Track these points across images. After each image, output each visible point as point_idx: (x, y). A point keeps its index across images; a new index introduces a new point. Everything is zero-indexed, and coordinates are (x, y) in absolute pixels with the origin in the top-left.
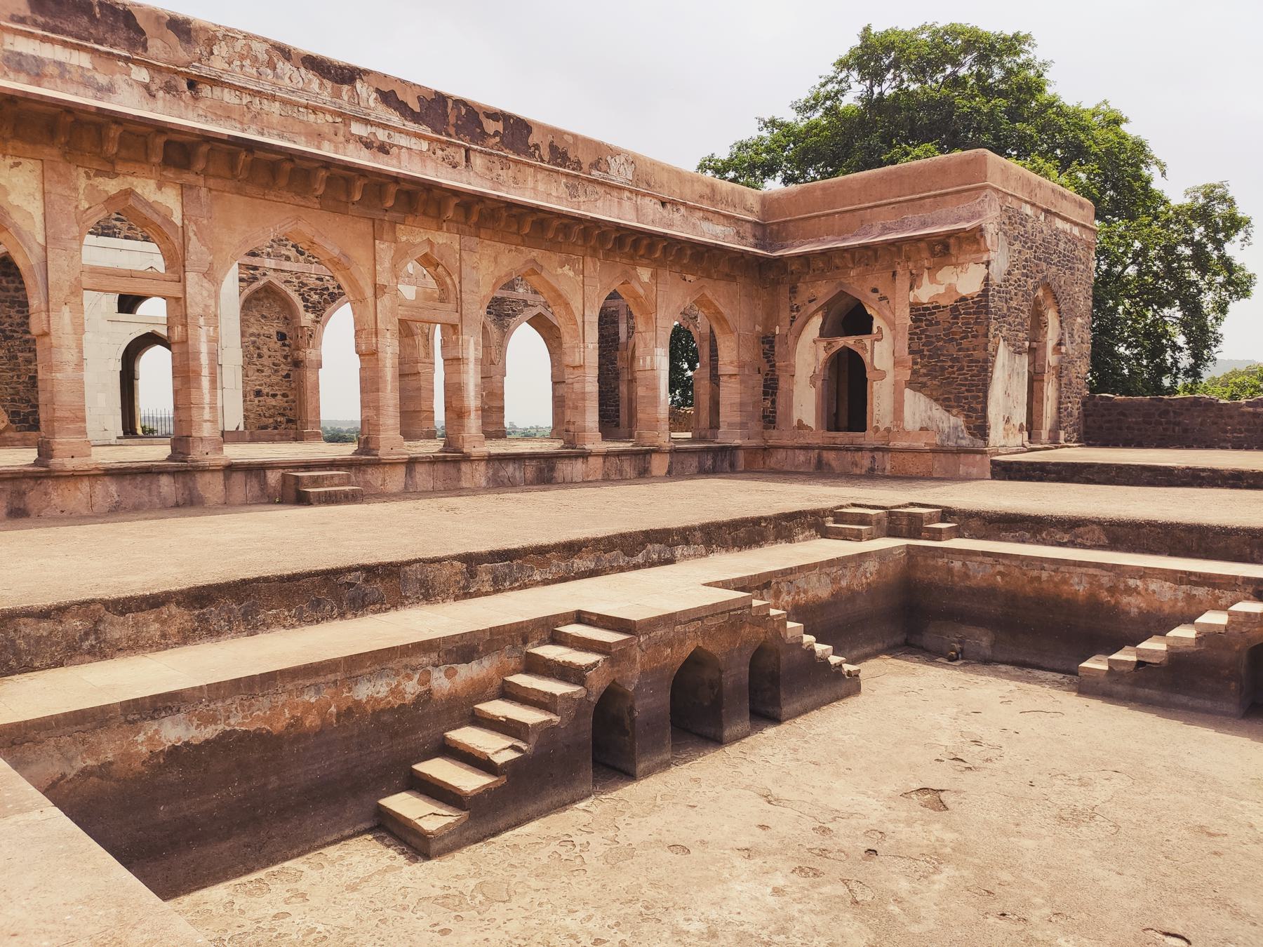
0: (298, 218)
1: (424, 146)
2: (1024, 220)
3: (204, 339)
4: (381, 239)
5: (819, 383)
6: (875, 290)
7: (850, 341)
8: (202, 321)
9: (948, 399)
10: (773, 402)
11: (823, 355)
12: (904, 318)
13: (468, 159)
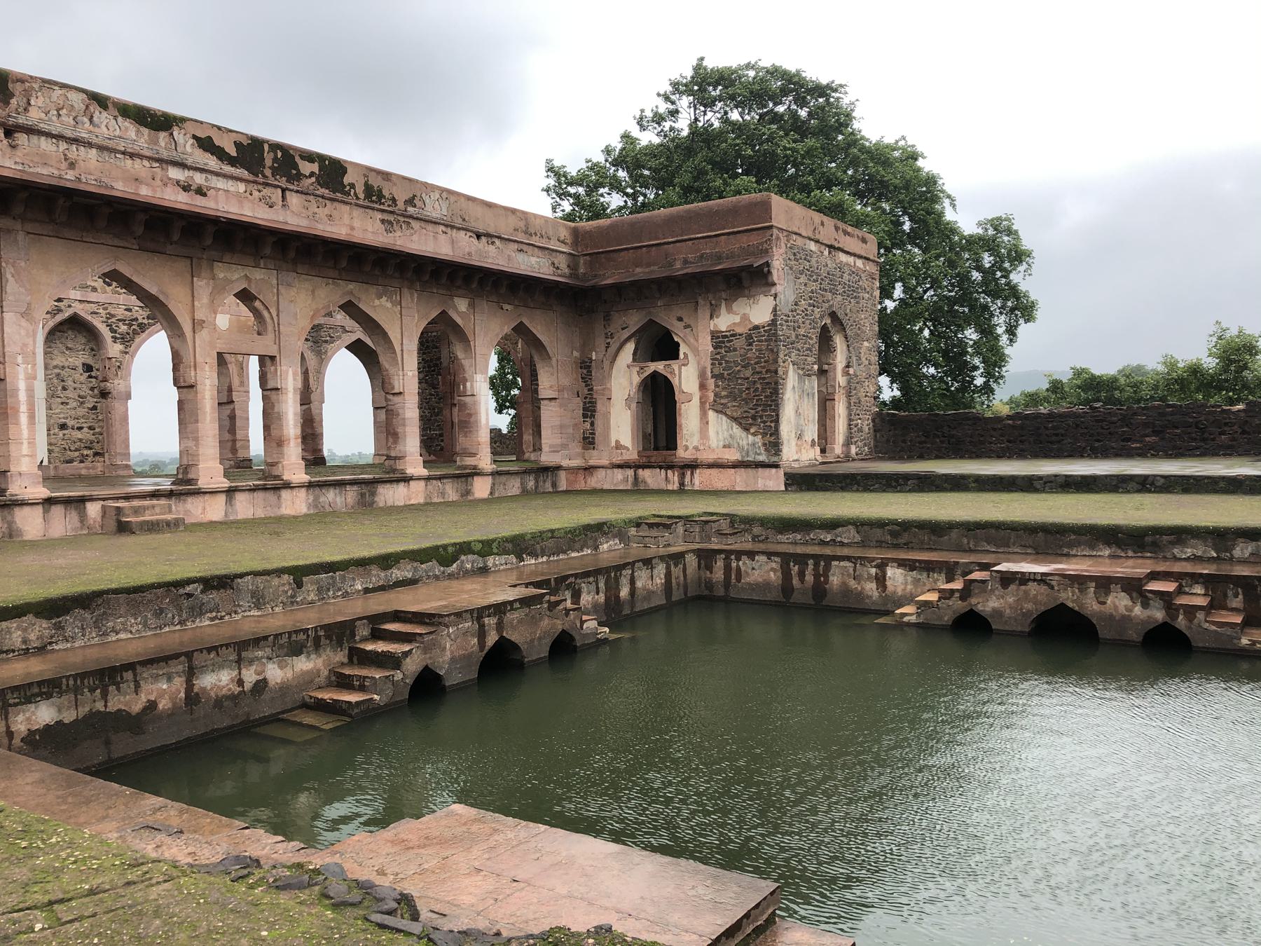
0: (116, 258)
1: (241, 187)
2: (808, 255)
3: (22, 376)
5: (634, 405)
6: (680, 319)
7: (659, 366)
8: (20, 359)
10: (592, 424)
11: (637, 380)
12: (706, 345)
13: (284, 198)
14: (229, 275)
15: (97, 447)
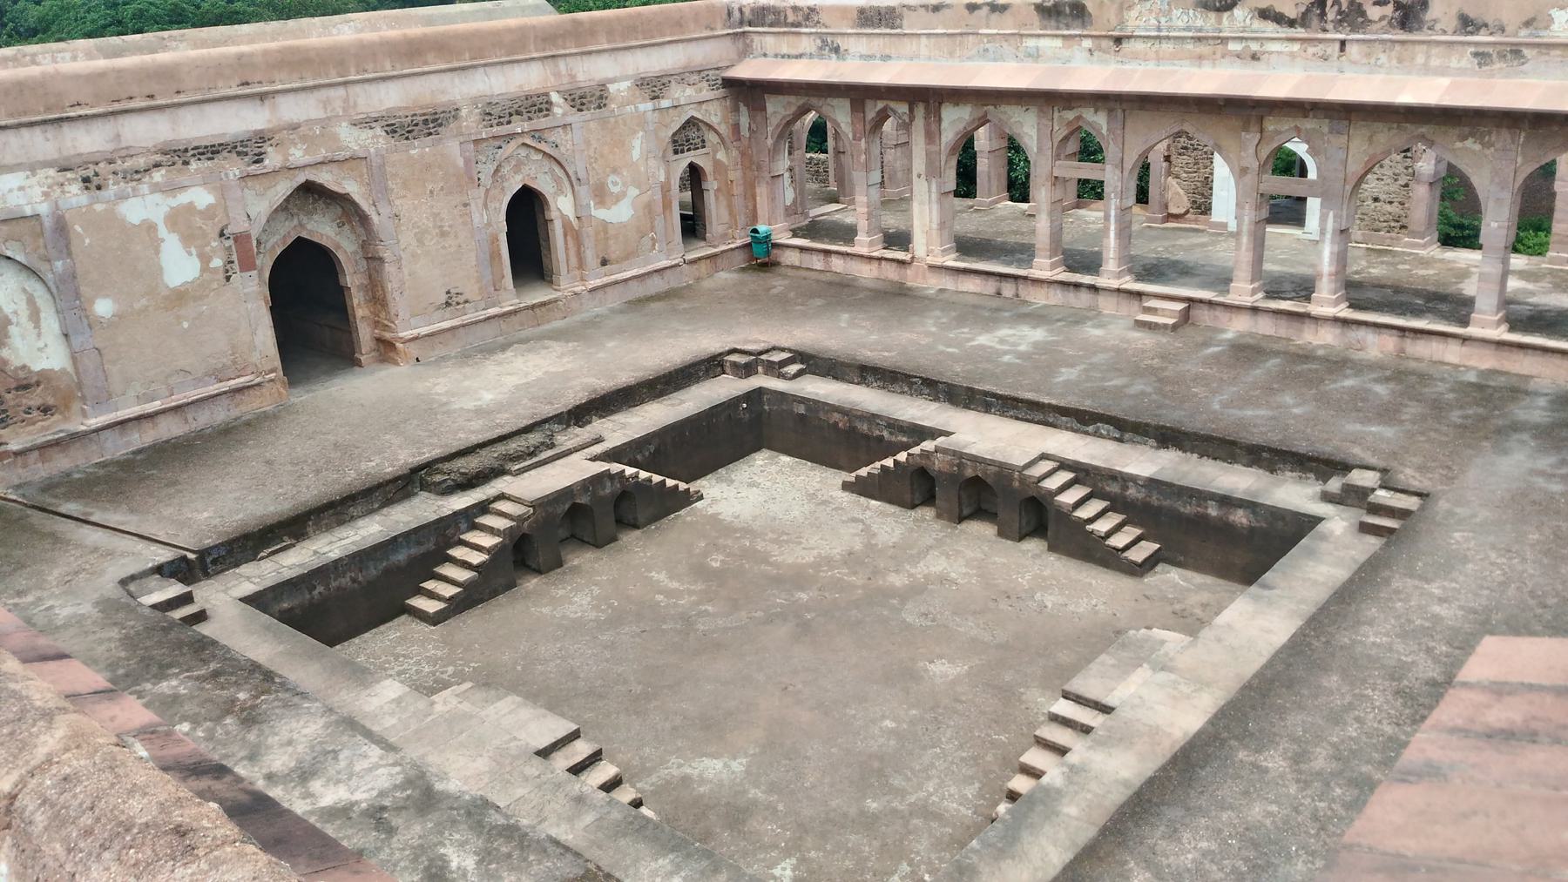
0: (1183, 121)
1: (1296, 47)
14: (1279, 127)
15: (1404, 221)
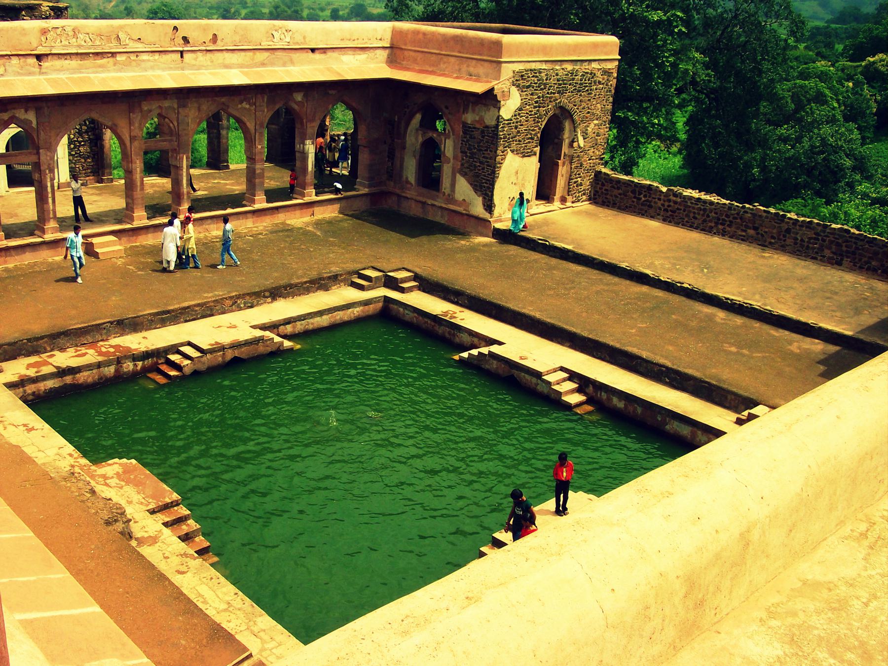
4: (134, 113)
9: (476, 185)
11: (420, 140)
